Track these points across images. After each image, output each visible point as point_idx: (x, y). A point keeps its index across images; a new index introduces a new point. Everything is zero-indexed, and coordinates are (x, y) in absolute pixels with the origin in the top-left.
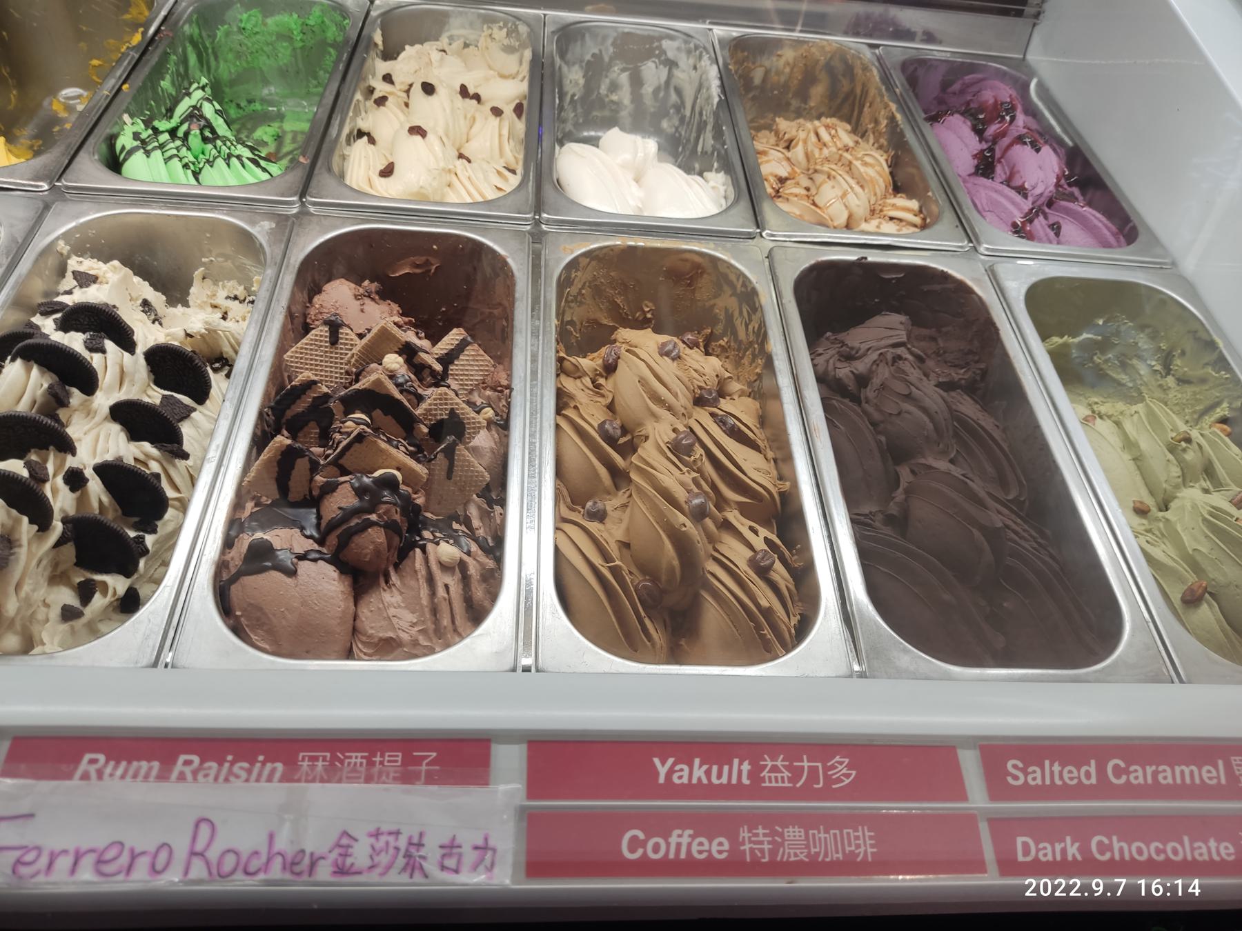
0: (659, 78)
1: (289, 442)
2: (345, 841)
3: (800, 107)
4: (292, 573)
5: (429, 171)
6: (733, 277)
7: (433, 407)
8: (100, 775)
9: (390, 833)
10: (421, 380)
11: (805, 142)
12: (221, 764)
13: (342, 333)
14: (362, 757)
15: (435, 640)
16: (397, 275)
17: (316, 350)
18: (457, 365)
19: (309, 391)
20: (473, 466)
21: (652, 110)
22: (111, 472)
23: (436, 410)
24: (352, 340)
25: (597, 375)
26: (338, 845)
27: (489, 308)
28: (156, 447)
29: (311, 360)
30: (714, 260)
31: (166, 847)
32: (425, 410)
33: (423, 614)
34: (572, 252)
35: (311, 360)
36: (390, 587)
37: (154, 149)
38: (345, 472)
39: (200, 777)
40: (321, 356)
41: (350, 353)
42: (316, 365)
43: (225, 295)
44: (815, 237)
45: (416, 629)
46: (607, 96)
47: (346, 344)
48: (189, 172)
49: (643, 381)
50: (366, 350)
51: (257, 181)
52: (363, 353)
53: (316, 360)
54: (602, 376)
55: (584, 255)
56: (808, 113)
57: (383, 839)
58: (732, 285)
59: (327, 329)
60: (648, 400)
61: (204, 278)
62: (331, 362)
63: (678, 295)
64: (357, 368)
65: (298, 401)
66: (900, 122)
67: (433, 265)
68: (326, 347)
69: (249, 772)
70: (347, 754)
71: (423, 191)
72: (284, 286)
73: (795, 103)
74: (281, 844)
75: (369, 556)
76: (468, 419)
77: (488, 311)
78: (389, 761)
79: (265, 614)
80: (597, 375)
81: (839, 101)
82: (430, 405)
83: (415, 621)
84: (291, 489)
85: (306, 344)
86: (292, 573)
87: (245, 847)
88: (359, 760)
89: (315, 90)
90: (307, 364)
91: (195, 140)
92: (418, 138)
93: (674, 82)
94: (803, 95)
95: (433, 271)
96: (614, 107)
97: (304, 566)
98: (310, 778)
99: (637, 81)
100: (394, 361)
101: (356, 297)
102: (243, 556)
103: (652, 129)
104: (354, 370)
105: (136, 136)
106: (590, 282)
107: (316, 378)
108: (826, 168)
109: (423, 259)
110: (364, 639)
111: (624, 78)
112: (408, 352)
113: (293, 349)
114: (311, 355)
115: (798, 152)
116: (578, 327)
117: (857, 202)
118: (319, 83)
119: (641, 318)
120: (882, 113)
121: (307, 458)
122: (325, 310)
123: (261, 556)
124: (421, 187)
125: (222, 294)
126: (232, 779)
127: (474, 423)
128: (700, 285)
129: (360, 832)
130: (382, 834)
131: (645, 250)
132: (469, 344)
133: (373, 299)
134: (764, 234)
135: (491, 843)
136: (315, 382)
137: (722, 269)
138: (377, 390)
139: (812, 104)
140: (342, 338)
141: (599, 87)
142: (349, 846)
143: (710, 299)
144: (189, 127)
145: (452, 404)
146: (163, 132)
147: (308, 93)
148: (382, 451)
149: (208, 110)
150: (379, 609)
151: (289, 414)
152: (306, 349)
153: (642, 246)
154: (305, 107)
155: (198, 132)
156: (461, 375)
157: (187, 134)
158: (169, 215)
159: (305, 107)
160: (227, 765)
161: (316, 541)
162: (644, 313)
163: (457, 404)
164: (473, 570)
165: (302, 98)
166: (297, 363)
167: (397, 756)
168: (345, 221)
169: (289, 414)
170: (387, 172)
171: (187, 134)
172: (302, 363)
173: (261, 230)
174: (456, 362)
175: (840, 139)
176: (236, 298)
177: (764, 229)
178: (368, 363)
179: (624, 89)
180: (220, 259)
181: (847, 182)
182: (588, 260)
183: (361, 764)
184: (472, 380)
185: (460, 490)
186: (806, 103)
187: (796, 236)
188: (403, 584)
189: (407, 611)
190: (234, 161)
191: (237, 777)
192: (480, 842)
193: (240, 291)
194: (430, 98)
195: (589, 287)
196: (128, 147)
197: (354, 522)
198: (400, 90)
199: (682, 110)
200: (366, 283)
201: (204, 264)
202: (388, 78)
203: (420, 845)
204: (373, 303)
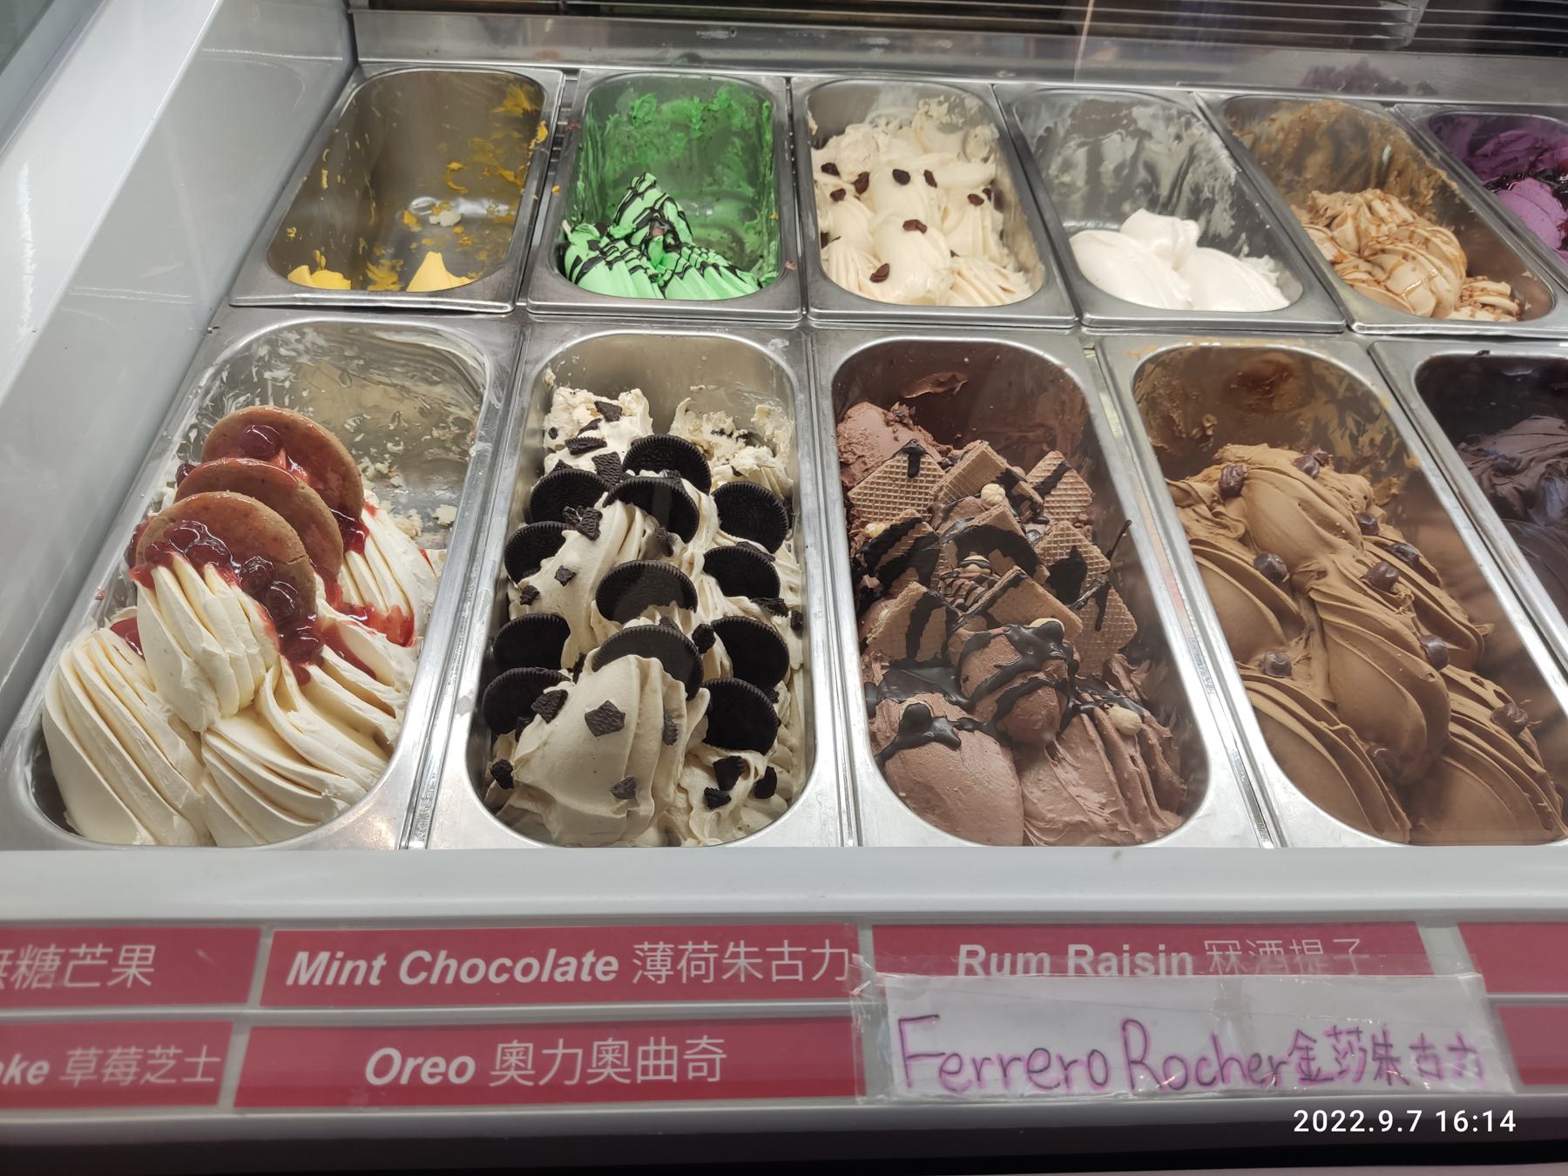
0: (1124, 153)
1: (924, 589)
2: (1302, 1042)
3: (1292, 180)
4: (954, 745)
5: (937, 271)
6: (1333, 380)
7: (1052, 545)
8: (986, 966)
9: (1349, 1032)
10: (1020, 514)
11: (1355, 218)
12: (1119, 953)
13: (924, 463)
14: (1277, 946)
15: (1132, 824)
16: (914, 396)
17: (890, 485)
18: (1053, 496)
19: (911, 531)
20: (1124, 614)
21: (1111, 191)
22: (729, 629)
23: (1055, 548)
24: (935, 470)
25: (1214, 501)
26: (1296, 1047)
27: (1021, 431)
28: (756, 602)
29: (883, 496)
30: (1307, 360)
31: (1096, 1054)
32: (1043, 549)
33: (1112, 793)
34: (1139, 358)
35: (883, 496)
36: (1059, 762)
37: (617, 259)
38: (993, 624)
39: (1101, 968)
40: (896, 491)
41: (936, 487)
42: (889, 503)
43: (711, 429)
44: (1418, 329)
45: (1107, 811)
46: (1057, 177)
47: (928, 476)
48: (655, 285)
49: (1305, 505)
50: (959, 481)
51: (742, 294)
52: (955, 486)
53: (889, 497)
54: (1219, 503)
55: (1151, 360)
56: (1302, 187)
57: (1344, 1039)
58: (1330, 390)
59: (905, 458)
60: (1317, 527)
61: (686, 411)
62: (907, 498)
63: (1251, 405)
64: (946, 503)
65: (897, 544)
66: (1458, 192)
67: (959, 381)
68: (903, 480)
69: (1155, 962)
70: (1258, 942)
71: (930, 295)
72: (826, 412)
73: (1287, 176)
74: (1231, 1046)
75: (1040, 724)
76: (1092, 558)
77: (1016, 435)
78: (1309, 950)
79: (938, 794)
80: (1214, 501)
81: (1346, 170)
82: (1049, 542)
83: (1104, 801)
84: (922, 647)
85: (879, 478)
86: (954, 745)
87: (1191, 1053)
88: (1274, 949)
89: (708, 189)
90: (877, 502)
91: (655, 249)
92: (918, 233)
93: (1144, 156)
94: (1297, 165)
95: (958, 389)
96: (1064, 190)
97: (964, 736)
98: (1228, 970)
99: (1095, 159)
100: (994, 492)
101: (888, 424)
102: (896, 725)
103: (1109, 215)
104: (943, 506)
105: (593, 245)
106: (1148, 394)
107: (918, 515)
108: (1400, 247)
109: (949, 375)
110: (1042, 824)
111: (1081, 156)
112: (1008, 481)
113: (862, 484)
114: (884, 490)
115: (1347, 231)
116: (1348, 432)
117: (1447, 286)
118: (714, 180)
119: (1198, 436)
120: (1424, 181)
121: (944, 608)
122: (854, 441)
123: (916, 727)
124: (929, 291)
125: (707, 428)
126: (1137, 971)
127: (1097, 564)
128: (1282, 392)
129: (1314, 1031)
130: (1340, 1033)
131: (1220, 351)
132: (1068, 469)
133: (905, 425)
134: (1354, 327)
135: (1469, 1042)
136: (919, 521)
137: (1317, 370)
138: (999, 526)
139: (1308, 176)
140: (923, 469)
141: (1049, 167)
142: (1308, 1049)
143: (1294, 409)
144: (650, 233)
145: (1074, 541)
146: (618, 240)
147: (701, 193)
148: (1038, 596)
149: (670, 212)
150: (1055, 788)
151: (885, 559)
152: (878, 484)
153: (1218, 348)
154: (695, 210)
155: (662, 238)
156: (1058, 507)
157: (646, 241)
158: (663, 336)
159: (695, 210)
160: (1126, 955)
161: (963, 707)
162: (1204, 429)
163: (1080, 541)
164: (1154, 740)
165: (692, 199)
166: (865, 500)
167: (1317, 944)
168: (866, 335)
169: (885, 559)
170: (881, 275)
171: (646, 241)
172: (871, 501)
173: (773, 350)
174: (1053, 493)
175: (1397, 213)
176: (722, 432)
177: (1353, 321)
178: (959, 498)
179: (1079, 168)
180: (711, 387)
181: (1432, 263)
182: (1153, 366)
183: (1279, 952)
184: (1068, 513)
185: (1107, 644)
186: (1300, 175)
187: (1394, 329)
188: (1076, 758)
189: (1090, 790)
190: (711, 270)
191: (1144, 970)
192: (1455, 1043)
193: (728, 424)
194: (905, 188)
195: (1146, 400)
196: (585, 259)
197: (1017, 683)
198: (847, 182)
199: (1154, 189)
200: (896, 406)
201: (690, 394)
202: (830, 169)
203: (1387, 1046)
204: (905, 429)
